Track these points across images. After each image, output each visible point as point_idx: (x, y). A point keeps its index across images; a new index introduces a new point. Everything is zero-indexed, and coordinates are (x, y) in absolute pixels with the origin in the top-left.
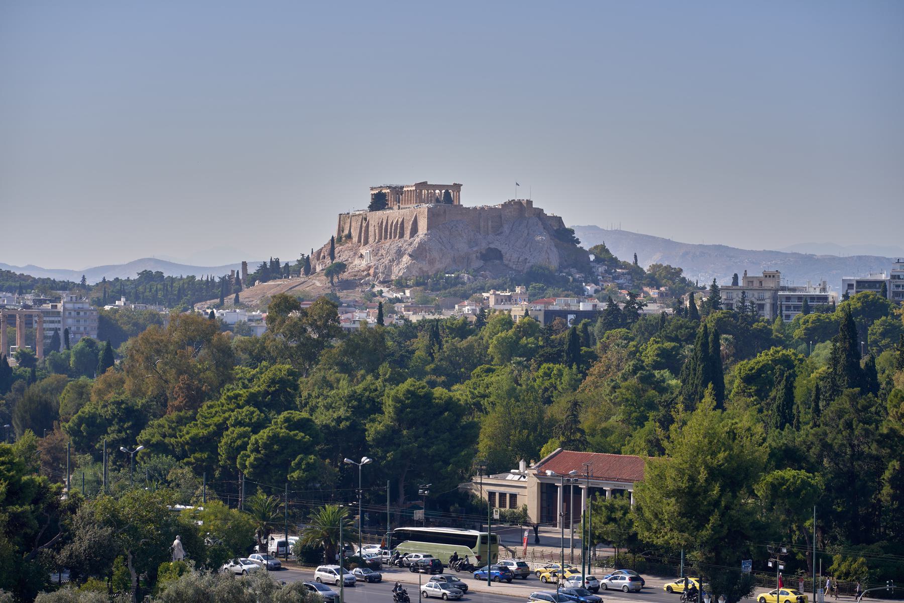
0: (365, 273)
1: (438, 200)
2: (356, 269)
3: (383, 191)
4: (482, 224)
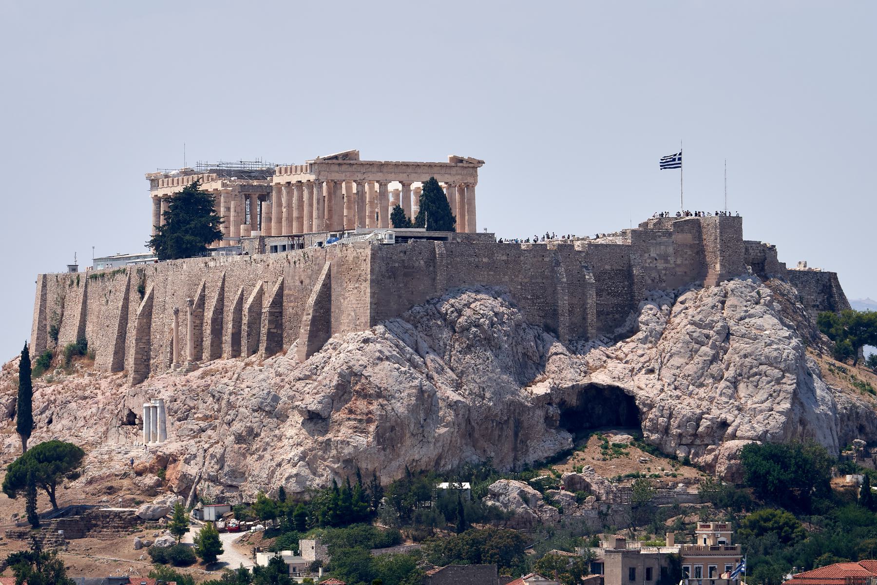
0: (150, 480)
1: (399, 218)
2: (118, 466)
3: (209, 186)
4: (564, 301)
